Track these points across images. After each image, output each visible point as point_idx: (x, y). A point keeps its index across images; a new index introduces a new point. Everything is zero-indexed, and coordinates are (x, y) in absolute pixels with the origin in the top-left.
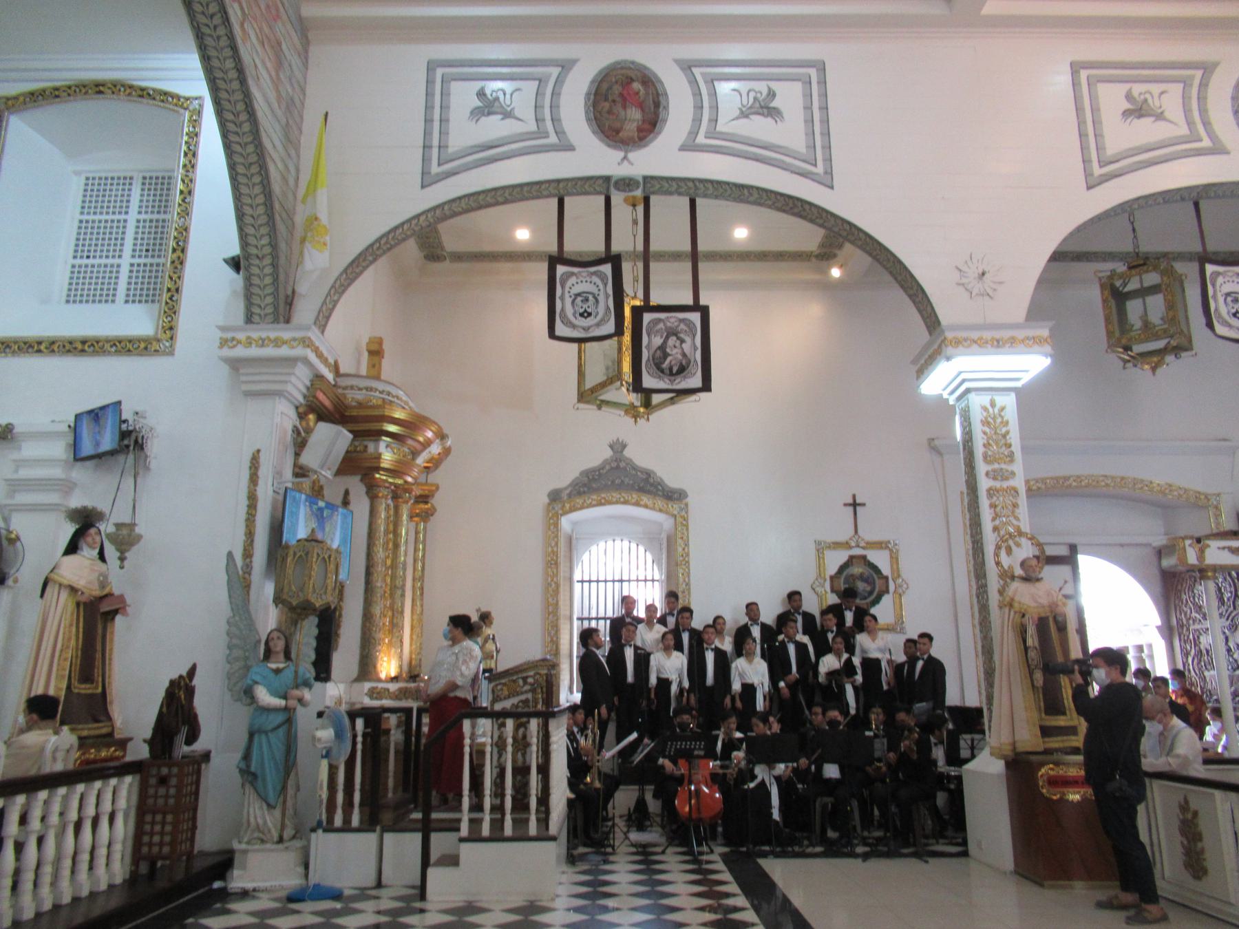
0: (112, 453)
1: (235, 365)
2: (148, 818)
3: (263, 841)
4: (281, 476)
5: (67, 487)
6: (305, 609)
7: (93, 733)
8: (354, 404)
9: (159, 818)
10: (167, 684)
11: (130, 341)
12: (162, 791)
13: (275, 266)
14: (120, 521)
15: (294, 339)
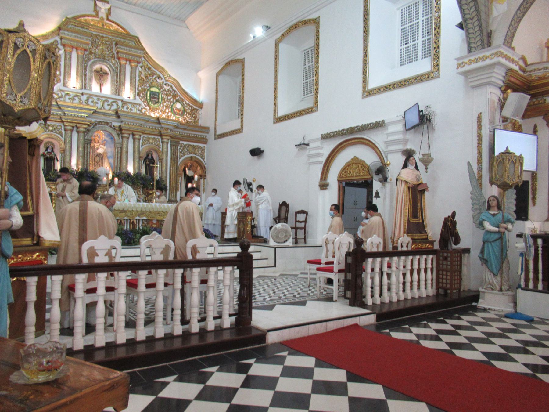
0: (417, 125)
1: (465, 74)
2: (441, 272)
3: (492, 289)
4: (494, 124)
5: (405, 141)
6: (505, 186)
7: (419, 237)
8: (536, 78)
9: (445, 273)
10: (443, 220)
11: (422, 76)
12: (445, 263)
13: (479, 20)
14: (423, 153)
15: (492, 54)
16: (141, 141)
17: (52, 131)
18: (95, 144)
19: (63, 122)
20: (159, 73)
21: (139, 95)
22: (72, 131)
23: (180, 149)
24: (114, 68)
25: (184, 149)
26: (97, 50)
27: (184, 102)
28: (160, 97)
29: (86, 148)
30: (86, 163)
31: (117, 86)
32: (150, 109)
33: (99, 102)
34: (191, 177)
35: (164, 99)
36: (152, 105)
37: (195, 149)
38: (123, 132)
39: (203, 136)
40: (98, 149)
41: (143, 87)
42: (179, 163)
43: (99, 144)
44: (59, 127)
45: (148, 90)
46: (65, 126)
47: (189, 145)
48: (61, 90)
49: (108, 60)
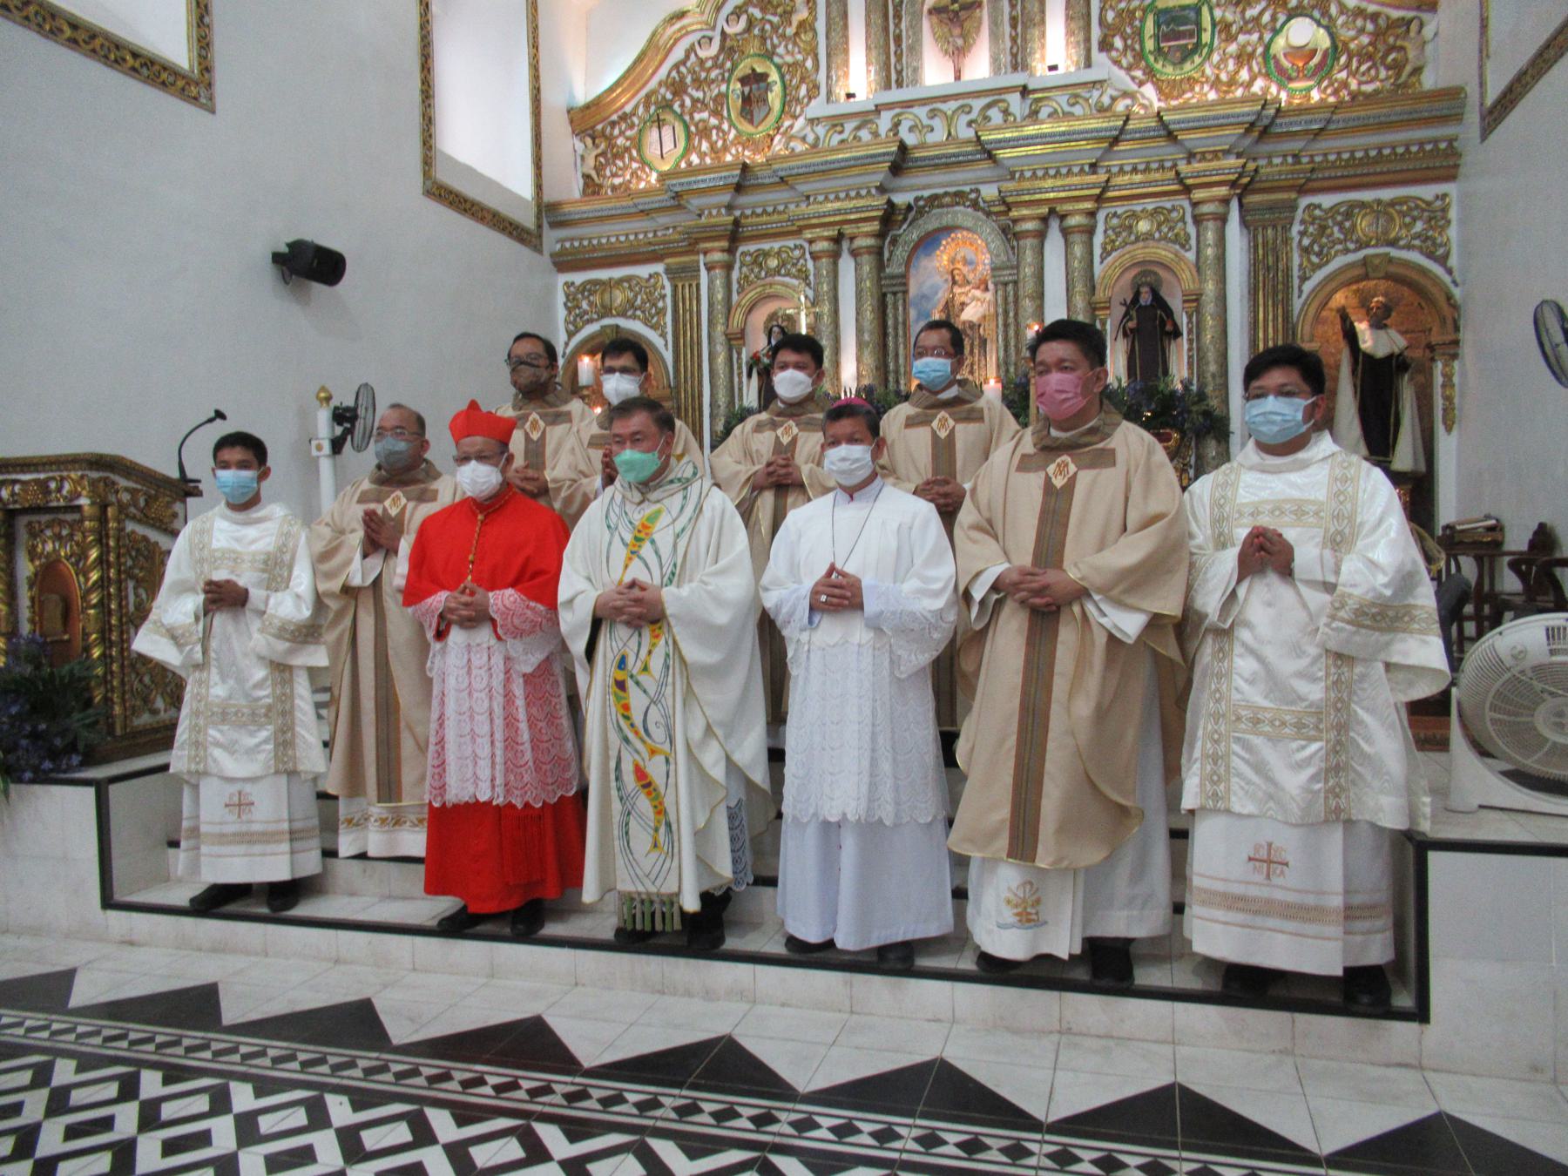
16: (1099, 239)
17: (777, 272)
18: (957, 290)
19: (799, 231)
21: (1105, 46)
22: (835, 256)
23: (1303, 234)
25: (1323, 229)
30: (892, 366)
31: (1014, 40)
32: (1159, 90)
33: (938, 123)
34: (1390, 357)
35: (1228, 26)
36: (1168, 72)
37: (1392, 219)
38: (1014, 213)
39: (1436, 141)
40: (963, 305)
41: (1123, 5)
42: (1297, 304)
43: (968, 288)
44: (797, 253)
45: (1144, 11)
46: (811, 242)
47: (1353, 206)
48: (812, 122)
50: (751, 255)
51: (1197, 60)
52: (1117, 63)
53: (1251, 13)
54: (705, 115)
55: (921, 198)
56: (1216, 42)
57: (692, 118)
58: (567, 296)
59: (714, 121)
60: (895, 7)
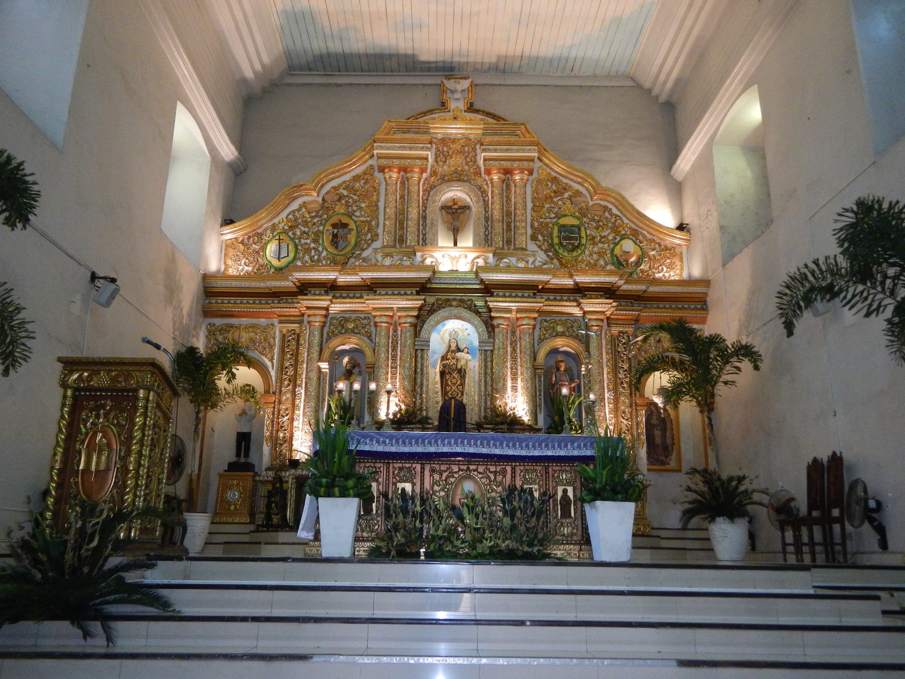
16: (537, 332)
20: (576, 187)
21: (534, 238)
24: (480, 194)
26: (445, 167)
27: (641, 238)
28: (583, 234)
29: (419, 359)
35: (593, 238)
38: (493, 314)
44: (365, 321)
49: (468, 181)
50: (337, 320)
51: (580, 251)
52: (540, 247)
53: (603, 234)
54: (308, 241)
55: (440, 299)
56: (588, 245)
57: (300, 241)
58: (209, 332)
59: (312, 245)
60: (423, 202)
